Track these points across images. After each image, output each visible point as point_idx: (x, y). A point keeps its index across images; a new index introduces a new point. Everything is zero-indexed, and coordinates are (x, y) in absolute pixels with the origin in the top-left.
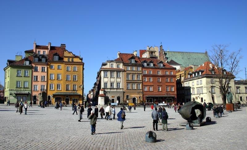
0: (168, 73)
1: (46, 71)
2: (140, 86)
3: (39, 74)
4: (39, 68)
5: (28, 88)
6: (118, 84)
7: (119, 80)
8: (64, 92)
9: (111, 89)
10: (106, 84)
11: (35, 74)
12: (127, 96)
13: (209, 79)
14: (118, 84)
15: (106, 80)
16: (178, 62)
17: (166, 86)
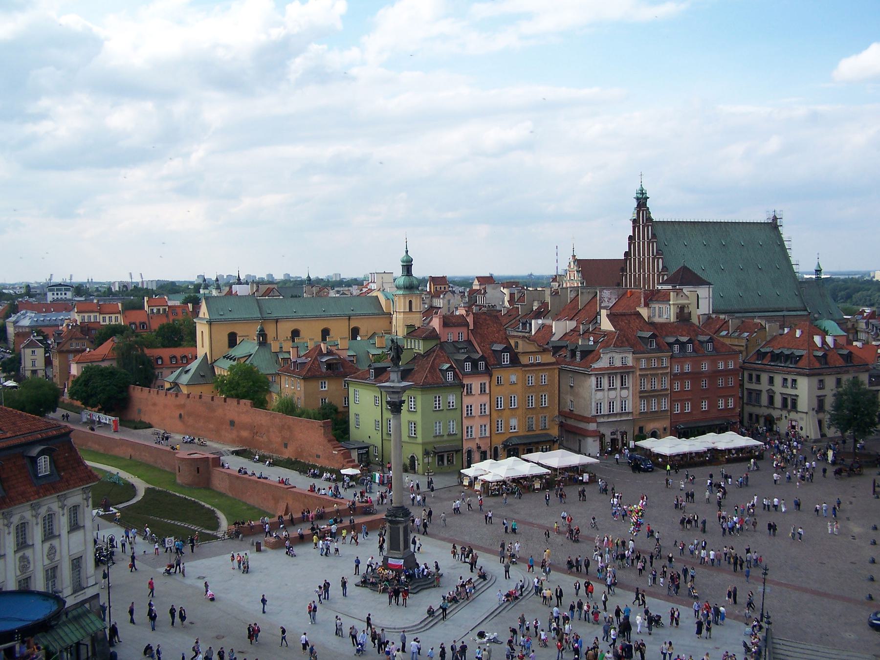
0: (721, 366)
1: (487, 391)
2: (665, 405)
3: (476, 401)
4: (475, 384)
5: (455, 434)
6: (623, 401)
7: (624, 393)
8: (522, 434)
9: (609, 415)
10: (599, 405)
11: (467, 401)
12: (641, 429)
13: (815, 380)
14: (623, 401)
15: (600, 395)
16: (704, 277)
17: (720, 397)
